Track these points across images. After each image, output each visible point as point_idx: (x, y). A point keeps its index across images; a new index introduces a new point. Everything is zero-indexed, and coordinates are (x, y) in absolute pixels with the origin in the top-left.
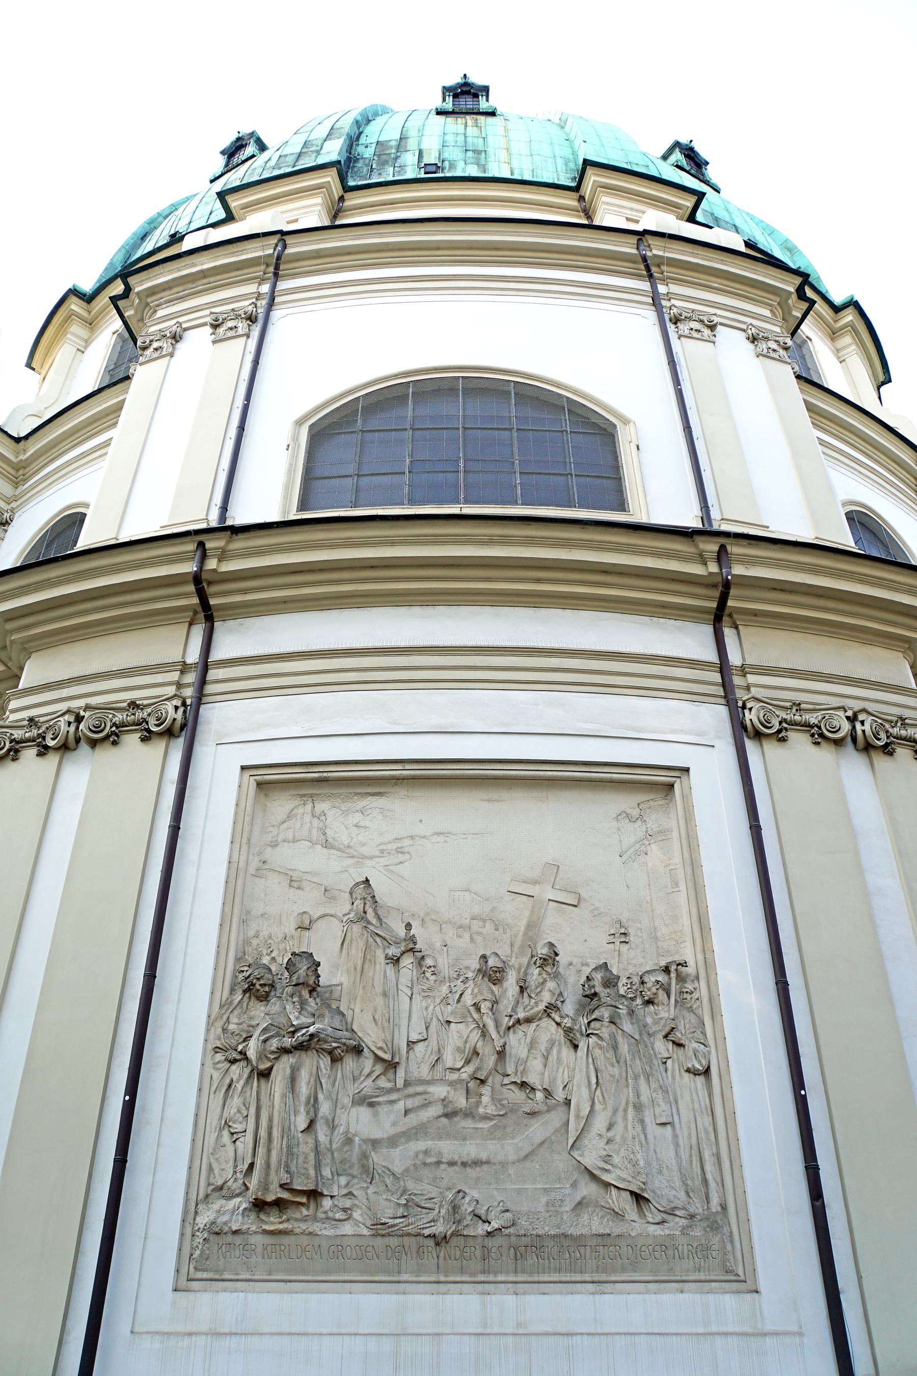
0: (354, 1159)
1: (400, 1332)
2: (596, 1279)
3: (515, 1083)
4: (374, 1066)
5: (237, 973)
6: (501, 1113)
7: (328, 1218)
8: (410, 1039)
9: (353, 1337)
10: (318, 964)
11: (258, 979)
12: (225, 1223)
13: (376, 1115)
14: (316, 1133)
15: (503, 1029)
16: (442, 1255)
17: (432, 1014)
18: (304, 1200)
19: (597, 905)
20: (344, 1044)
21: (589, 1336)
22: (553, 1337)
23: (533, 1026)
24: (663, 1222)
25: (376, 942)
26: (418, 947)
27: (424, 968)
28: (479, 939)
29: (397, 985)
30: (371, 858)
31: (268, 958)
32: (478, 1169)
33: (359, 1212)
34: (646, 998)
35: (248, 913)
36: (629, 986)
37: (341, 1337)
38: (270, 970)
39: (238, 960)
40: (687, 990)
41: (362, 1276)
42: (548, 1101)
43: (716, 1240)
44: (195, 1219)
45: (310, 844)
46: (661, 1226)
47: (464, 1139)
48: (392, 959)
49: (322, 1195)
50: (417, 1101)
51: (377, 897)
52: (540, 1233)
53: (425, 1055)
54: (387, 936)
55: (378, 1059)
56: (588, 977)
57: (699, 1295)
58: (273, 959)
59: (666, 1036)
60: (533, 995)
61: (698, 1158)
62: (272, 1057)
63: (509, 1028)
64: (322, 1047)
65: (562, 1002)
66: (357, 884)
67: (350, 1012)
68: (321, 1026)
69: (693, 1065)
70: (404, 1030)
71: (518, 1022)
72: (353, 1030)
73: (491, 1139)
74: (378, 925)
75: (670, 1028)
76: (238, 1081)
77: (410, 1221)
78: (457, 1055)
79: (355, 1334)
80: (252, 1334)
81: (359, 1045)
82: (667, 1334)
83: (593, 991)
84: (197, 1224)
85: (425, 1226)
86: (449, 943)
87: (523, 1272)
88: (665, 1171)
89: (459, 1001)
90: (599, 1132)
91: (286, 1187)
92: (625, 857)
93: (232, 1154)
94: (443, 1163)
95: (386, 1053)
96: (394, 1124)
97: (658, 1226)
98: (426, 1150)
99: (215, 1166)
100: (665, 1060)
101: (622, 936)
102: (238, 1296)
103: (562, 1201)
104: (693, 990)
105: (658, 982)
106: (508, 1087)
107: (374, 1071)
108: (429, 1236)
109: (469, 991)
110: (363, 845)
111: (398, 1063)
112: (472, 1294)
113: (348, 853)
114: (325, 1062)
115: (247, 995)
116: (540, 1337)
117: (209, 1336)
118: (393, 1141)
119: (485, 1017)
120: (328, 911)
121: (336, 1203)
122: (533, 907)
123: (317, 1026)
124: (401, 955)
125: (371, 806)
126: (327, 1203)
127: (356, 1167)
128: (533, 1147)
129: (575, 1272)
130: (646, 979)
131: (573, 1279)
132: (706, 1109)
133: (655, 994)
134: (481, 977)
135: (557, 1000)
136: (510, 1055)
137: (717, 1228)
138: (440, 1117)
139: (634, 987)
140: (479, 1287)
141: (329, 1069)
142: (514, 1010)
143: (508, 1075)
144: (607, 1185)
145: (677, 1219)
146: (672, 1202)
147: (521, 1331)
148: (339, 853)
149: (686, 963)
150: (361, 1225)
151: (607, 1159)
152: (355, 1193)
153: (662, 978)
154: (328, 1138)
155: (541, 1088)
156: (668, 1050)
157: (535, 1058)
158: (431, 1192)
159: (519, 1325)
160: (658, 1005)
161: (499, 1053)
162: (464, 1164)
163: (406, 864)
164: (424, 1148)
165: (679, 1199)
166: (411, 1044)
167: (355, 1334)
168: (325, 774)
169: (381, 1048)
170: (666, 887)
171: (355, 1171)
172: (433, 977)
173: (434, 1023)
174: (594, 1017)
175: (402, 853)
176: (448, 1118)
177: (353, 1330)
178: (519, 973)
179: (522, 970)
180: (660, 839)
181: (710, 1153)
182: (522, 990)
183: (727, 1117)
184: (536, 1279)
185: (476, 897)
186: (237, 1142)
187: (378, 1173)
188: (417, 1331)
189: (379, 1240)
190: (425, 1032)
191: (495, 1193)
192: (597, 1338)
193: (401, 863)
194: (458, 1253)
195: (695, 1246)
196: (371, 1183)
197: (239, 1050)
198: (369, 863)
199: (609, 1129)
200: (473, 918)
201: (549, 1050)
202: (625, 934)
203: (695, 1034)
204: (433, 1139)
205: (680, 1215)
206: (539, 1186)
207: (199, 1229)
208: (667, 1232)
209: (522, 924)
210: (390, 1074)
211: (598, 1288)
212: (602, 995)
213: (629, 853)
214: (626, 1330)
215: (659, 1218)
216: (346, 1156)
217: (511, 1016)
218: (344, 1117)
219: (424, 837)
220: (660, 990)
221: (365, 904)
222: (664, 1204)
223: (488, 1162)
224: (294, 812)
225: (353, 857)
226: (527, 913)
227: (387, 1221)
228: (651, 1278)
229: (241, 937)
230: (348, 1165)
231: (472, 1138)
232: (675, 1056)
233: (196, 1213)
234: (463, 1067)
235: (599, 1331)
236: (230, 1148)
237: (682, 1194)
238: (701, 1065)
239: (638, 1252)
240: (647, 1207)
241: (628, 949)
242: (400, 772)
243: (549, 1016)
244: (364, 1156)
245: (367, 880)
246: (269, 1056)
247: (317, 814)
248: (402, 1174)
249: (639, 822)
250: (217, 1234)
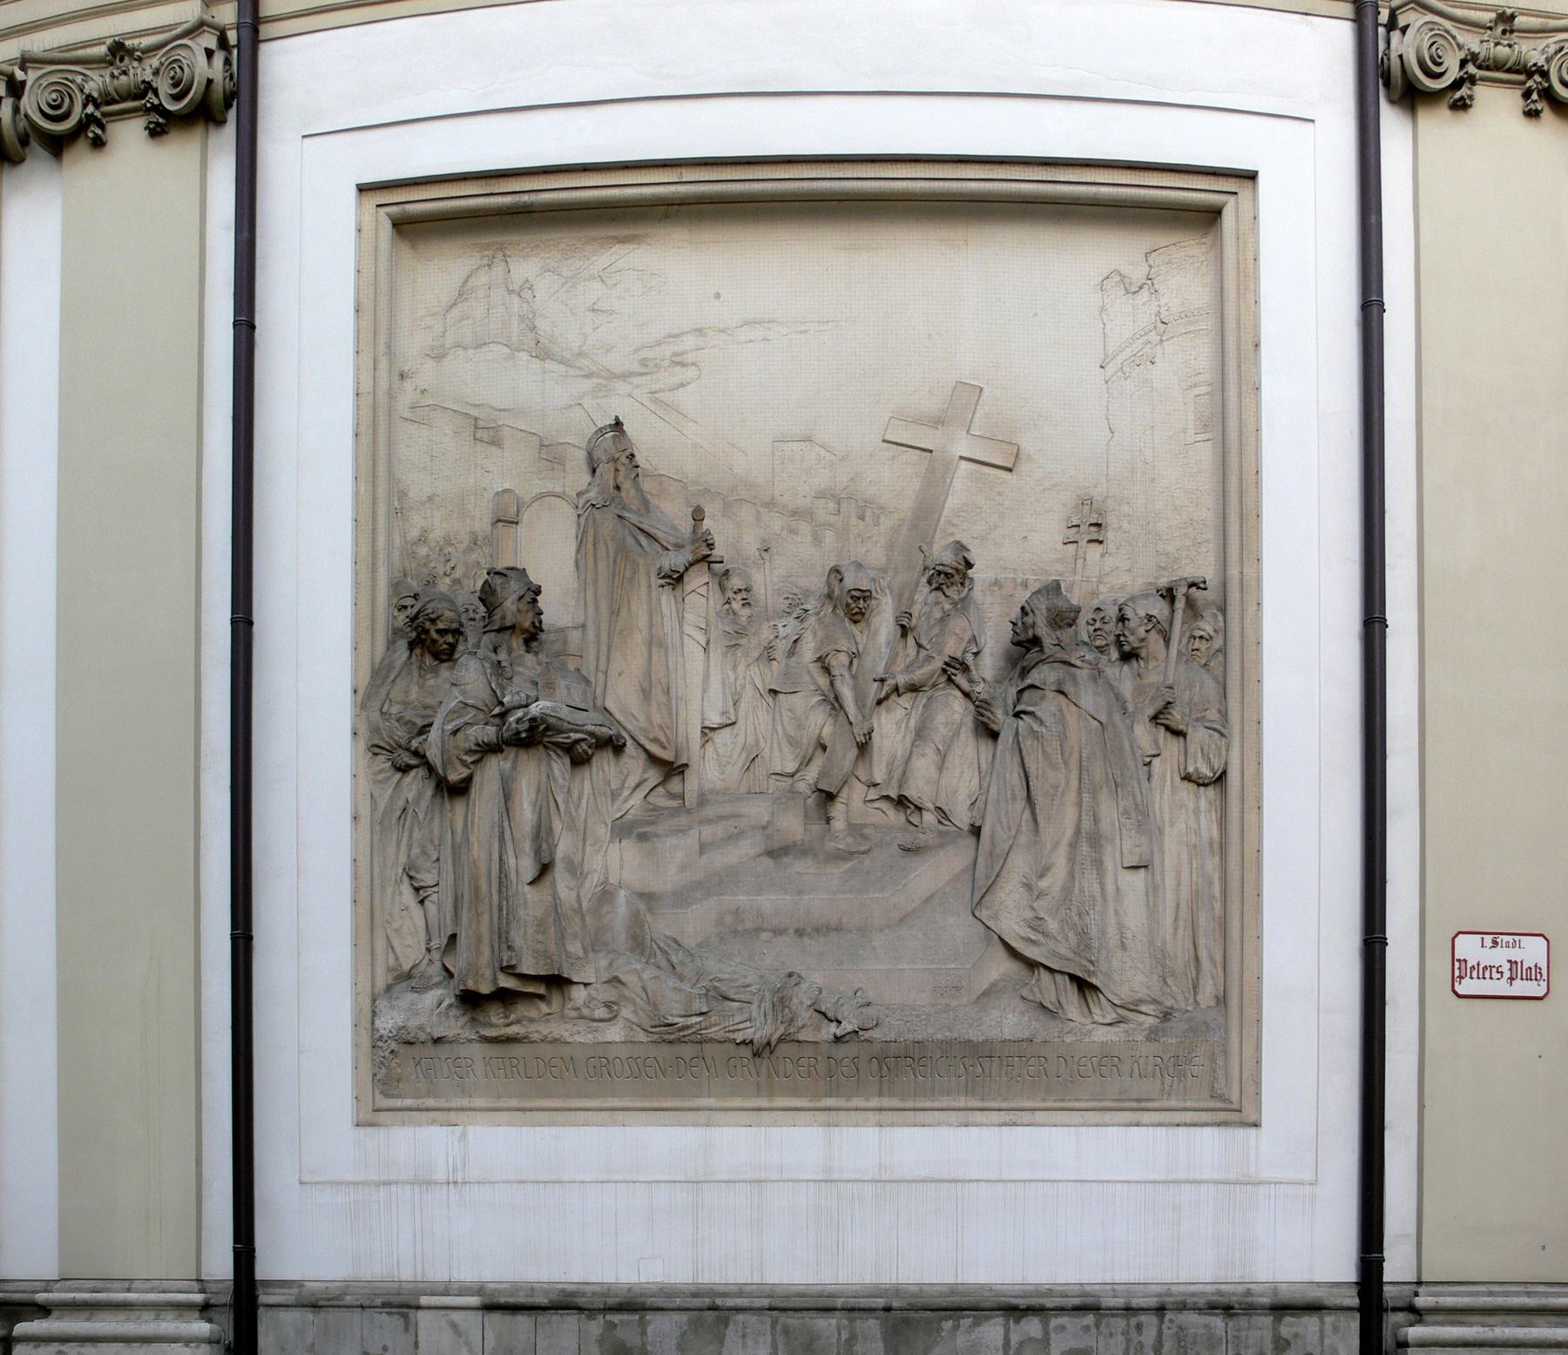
3: (887, 798)
4: (644, 771)
5: (396, 613)
8: (707, 724)
10: (538, 591)
11: (433, 621)
12: (421, 1028)
15: (871, 701)
17: (745, 678)
18: (542, 990)
20: (592, 734)
23: (922, 699)
26: (717, 553)
27: (730, 594)
28: (829, 537)
29: (681, 626)
30: (624, 377)
31: (447, 580)
33: (631, 1008)
34: (1127, 648)
35: (403, 494)
36: (1098, 625)
38: (451, 602)
39: (395, 586)
42: (941, 828)
44: (373, 1023)
45: (506, 350)
48: (670, 577)
49: (569, 982)
51: (639, 459)
52: (920, 1038)
53: (732, 750)
55: (653, 759)
56: (1023, 608)
58: (457, 582)
60: (924, 642)
62: (470, 759)
63: (879, 702)
64: (553, 740)
65: (976, 654)
66: (601, 431)
67: (601, 676)
68: (549, 704)
70: (695, 706)
72: (605, 709)
75: (1163, 703)
76: (417, 801)
77: (712, 1019)
78: (786, 749)
83: (1031, 633)
84: (378, 1030)
85: (736, 1027)
87: (891, 1095)
89: (791, 652)
90: (1025, 880)
91: (511, 971)
93: (421, 923)
94: (764, 931)
95: (664, 748)
97: (1110, 1028)
99: (395, 942)
101: (1092, 529)
105: (1150, 617)
106: (877, 805)
107: (645, 780)
108: (744, 1042)
109: (808, 636)
111: (686, 765)
112: (812, 1126)
114: (560, 766)
115: (418, 651)
119: (838, 683)
120: (549, 486)
123: (542, 703)
124: (687, 569)
126: (578, 994)
130: (1129, 613)
133: (1142, 640)
135: (965, 652)
136: (880, 749)
138: (759, 856)
139: (1106, 627)
141: (567, 777)
142: (887, 670)
143: (875, 785)
144: (1032, 965)
145: (1142, 1018)
148: (562, 368)
149: (1204, 582)
150: (635, 1027)
151: (1036, 924)
153: (1159, 608)
154: (574, 894)
155: (932, 807)
156: (1156, 742)
157: (923, 755)
158: (745, 977)
166: (707, 731)
170: (1185, 431)
172: (746, 612)
173: (748, 696)
174: (1028, 681)
175: (683, 364)
176: (772, 858)
179: (906, 596)
182: (905, 631)
186: (426, 902)
190: (732, 710)
197: (413, 748)
198: (622, 387)
199: (1041, 876)
200: (820, 495)
202: (1098, 525)
206: (920, 966)
207: (381, 1037)
209: (907, 505)
210: (675, 785)
212: (1048, 641)
213: (1119, 360)
221: (617, 470)
223: (838, 929)
225: (589, 376)
226: (916, 484)
227: (677, 1020)
229: (397, 541)
233: (374, 1013)
234: (798, 771)
236: (416, 911)
239: (1075, 1067)
240: (1095, 998)
241: (1103, 556)
242: (672, 189)
243: (950, 680)
245: (618, 424)
246: (464, 757)
247: (517, 288)
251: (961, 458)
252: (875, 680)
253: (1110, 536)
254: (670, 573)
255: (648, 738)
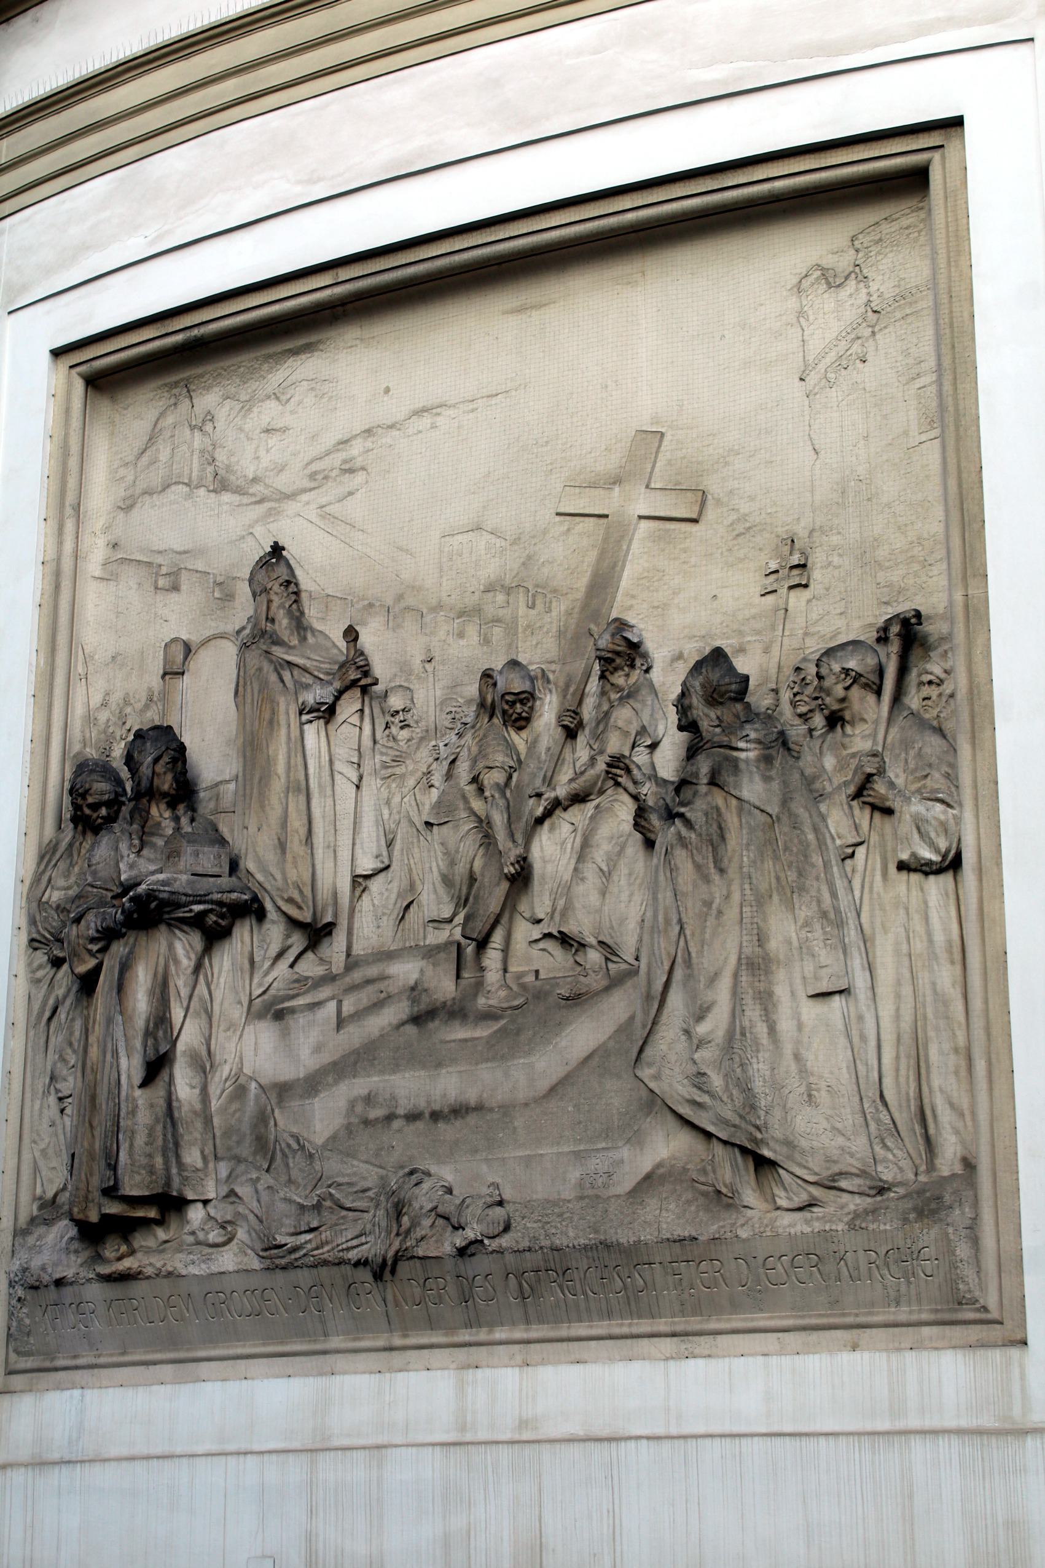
0: (246, 1128)
1: (318, 1446)
2: (679, 1328)
6: (516, 1003)
7: (198, 1243)
9: (242, 1458)
13: (285, 1034)
14: (171, 1082)
16: (390, 1297)
19: (745, 508)
21: (651, 1443)
22: (582, 1445)
24: (811, 1205)
25: (282, 681)
32: (458, 1123)
37: (223, 1458)
40: (930, 677)
41: (264, 1345)
43: (928, 1236)
46: (806, 1214)
47: (439, 1065)
48: (318, 710)
50: (365, 997)
54: (308, 664)
57: (884, 1355)
59: (858, 794)
61: (913, 1062)
63: (540, 821)
69: (914, 855)
71: (556, 805)
73: (487, 1060)
74: (295, 642)
79: (246, 1453)
80: (90, 1461)
81: (255, 899)
82: (807, 1435)
86: (436, 654)
88: (822, 1097)
92: (812, 379)
96: (318, 1049)
98: (369, 1094)
100: (850, 850)
101: (795, 572)
102: (71, 1396)
103: (609, 1175)
104: (943, 676)
110: (281, 469)
113: (253, 495)
116: (558, 1446)
117: (30, 1468)
118: (312, 1084)
121: (212, 1212)
122: (605, 540)
125: (293, 378)
126: (196, 1214)
127: (248, 1140)
128: (569, 1068)
129: (640, 1317)
131: (635, 1330)
132: (950, 951)
134: (486, 720)
137: (934, 1212)
140: (461, 1354)
144: (708, 1135)
145: (846, 1197)
146: (835, 1162)
147: (526, 1436)
152: (239, 1190)
159: (523, 1424)
160: (852, 723)
161: (512, 879)
162: (436, 1116)
163: (358, 495)
164: (364, 1092)
165: (852, 1155)
167: (246, 1453)
168: (195, 332)
169: (290, 900)
170: (906, 433)
171: (245, 1151)
177: (244, 1446)
178: (565, 697)
179: (572, 690)
180: (898, 315)
181: (946, 1046)
182: (571, 734)
183: (989, 964)
184: (564, 1332)
185: (493, 539)
187: (282, 1150)
188: (346, 1442)
189: (280, 1277)
191: (484, 1168)
192: (666, 1445)
193: (351, 494)
194: (417, 1291)
195: (882, 1251)
196: (268, 1171)
201: (613, 861)
203: (928, 781)
204: (382, 1072)
205: (850, 1189)
206: (566, 1149)
208: (817, 1226)
211: (683, 1346)
214: (727, 1429)
215: (802, 1198)
216: (233, 1122)
217: (539, 795)
218: (231, 1046)
219: (391, 427)
220: (855, 688)
222: (817, 1167)
223: (479, 1108)
224: (159, 426)
226: (592, 556)
228: (790, 1322)
230: (235, 1138)
231: (454, 1061)
232: (874, 838)
235: (674, 1431)
237: (861, 1145)
238: (937, 851)
244: (262, 1118)
248: (324, 1146)
249: (852, 283)
250: (36, 1288)
251: (640, 517)
252: (531, 797)
253: (818, 575)
254: (317, 706)
255: (283, 898)
